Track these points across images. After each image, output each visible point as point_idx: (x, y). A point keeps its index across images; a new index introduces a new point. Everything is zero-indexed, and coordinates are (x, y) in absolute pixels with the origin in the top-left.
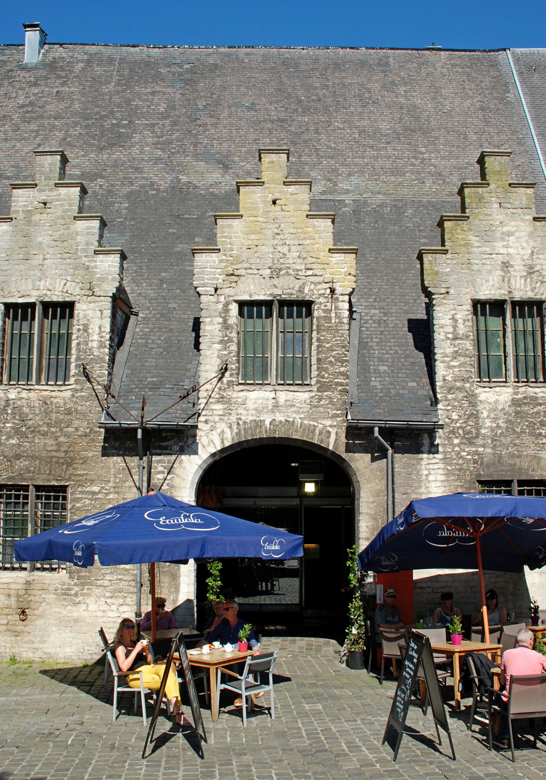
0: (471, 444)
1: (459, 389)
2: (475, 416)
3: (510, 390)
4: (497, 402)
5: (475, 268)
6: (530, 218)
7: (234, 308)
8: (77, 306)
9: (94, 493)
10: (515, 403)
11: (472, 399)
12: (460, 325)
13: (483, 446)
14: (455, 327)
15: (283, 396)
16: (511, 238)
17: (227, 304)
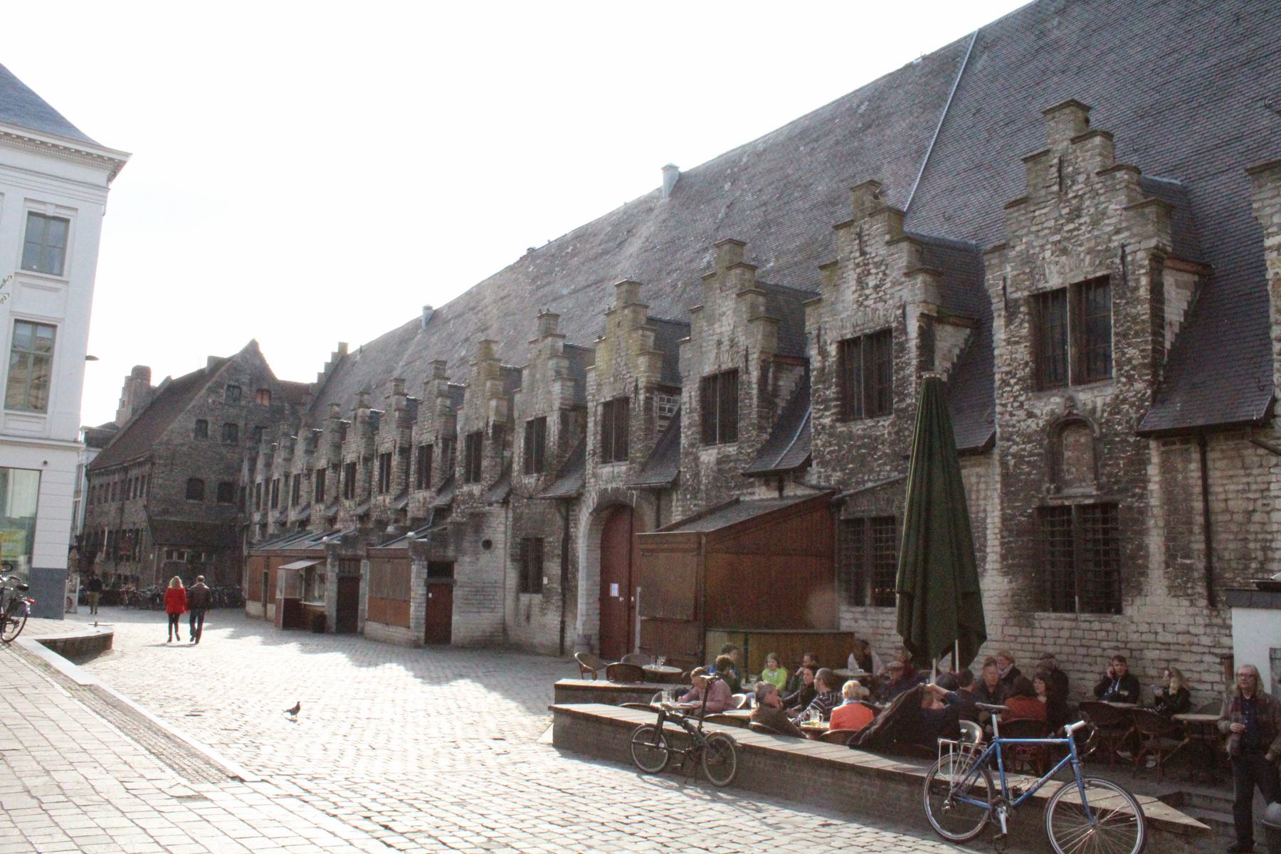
0: (696, 498)
1: (691, 453)
2: (696, 475)
3: (716, 451)
4: (709, 463)
5: (704, 349)
6: (734, 296)
7: (600, 409)
8: (548, 419)
9: (550, 542)
10: (719, 462)
11: (696, 459)
12: (693, 401)
13: (701, 499)
14: (691, 404)
15: (616, 470)
16: (724, 318)
17: (596, 406)
